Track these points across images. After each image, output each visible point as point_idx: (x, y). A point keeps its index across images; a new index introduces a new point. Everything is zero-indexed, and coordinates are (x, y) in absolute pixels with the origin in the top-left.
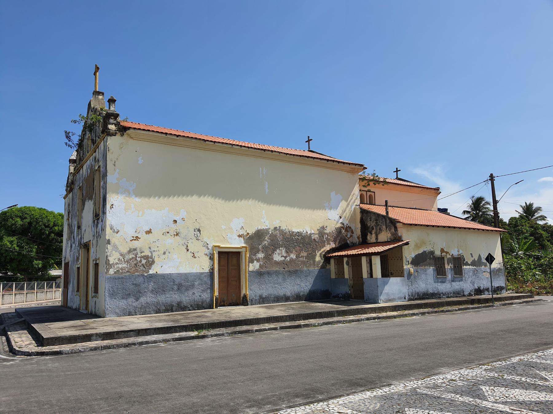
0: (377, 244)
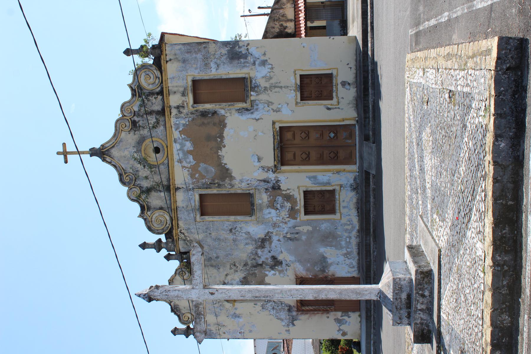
0: (296, 20)
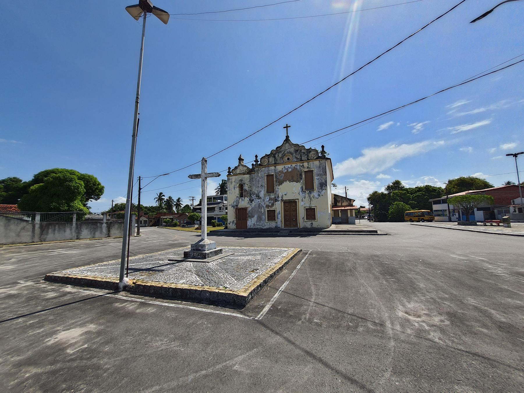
0: (342, 206)
